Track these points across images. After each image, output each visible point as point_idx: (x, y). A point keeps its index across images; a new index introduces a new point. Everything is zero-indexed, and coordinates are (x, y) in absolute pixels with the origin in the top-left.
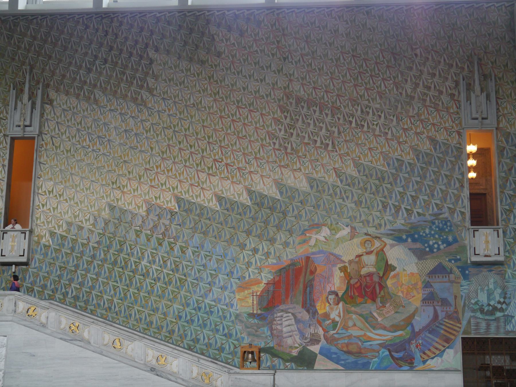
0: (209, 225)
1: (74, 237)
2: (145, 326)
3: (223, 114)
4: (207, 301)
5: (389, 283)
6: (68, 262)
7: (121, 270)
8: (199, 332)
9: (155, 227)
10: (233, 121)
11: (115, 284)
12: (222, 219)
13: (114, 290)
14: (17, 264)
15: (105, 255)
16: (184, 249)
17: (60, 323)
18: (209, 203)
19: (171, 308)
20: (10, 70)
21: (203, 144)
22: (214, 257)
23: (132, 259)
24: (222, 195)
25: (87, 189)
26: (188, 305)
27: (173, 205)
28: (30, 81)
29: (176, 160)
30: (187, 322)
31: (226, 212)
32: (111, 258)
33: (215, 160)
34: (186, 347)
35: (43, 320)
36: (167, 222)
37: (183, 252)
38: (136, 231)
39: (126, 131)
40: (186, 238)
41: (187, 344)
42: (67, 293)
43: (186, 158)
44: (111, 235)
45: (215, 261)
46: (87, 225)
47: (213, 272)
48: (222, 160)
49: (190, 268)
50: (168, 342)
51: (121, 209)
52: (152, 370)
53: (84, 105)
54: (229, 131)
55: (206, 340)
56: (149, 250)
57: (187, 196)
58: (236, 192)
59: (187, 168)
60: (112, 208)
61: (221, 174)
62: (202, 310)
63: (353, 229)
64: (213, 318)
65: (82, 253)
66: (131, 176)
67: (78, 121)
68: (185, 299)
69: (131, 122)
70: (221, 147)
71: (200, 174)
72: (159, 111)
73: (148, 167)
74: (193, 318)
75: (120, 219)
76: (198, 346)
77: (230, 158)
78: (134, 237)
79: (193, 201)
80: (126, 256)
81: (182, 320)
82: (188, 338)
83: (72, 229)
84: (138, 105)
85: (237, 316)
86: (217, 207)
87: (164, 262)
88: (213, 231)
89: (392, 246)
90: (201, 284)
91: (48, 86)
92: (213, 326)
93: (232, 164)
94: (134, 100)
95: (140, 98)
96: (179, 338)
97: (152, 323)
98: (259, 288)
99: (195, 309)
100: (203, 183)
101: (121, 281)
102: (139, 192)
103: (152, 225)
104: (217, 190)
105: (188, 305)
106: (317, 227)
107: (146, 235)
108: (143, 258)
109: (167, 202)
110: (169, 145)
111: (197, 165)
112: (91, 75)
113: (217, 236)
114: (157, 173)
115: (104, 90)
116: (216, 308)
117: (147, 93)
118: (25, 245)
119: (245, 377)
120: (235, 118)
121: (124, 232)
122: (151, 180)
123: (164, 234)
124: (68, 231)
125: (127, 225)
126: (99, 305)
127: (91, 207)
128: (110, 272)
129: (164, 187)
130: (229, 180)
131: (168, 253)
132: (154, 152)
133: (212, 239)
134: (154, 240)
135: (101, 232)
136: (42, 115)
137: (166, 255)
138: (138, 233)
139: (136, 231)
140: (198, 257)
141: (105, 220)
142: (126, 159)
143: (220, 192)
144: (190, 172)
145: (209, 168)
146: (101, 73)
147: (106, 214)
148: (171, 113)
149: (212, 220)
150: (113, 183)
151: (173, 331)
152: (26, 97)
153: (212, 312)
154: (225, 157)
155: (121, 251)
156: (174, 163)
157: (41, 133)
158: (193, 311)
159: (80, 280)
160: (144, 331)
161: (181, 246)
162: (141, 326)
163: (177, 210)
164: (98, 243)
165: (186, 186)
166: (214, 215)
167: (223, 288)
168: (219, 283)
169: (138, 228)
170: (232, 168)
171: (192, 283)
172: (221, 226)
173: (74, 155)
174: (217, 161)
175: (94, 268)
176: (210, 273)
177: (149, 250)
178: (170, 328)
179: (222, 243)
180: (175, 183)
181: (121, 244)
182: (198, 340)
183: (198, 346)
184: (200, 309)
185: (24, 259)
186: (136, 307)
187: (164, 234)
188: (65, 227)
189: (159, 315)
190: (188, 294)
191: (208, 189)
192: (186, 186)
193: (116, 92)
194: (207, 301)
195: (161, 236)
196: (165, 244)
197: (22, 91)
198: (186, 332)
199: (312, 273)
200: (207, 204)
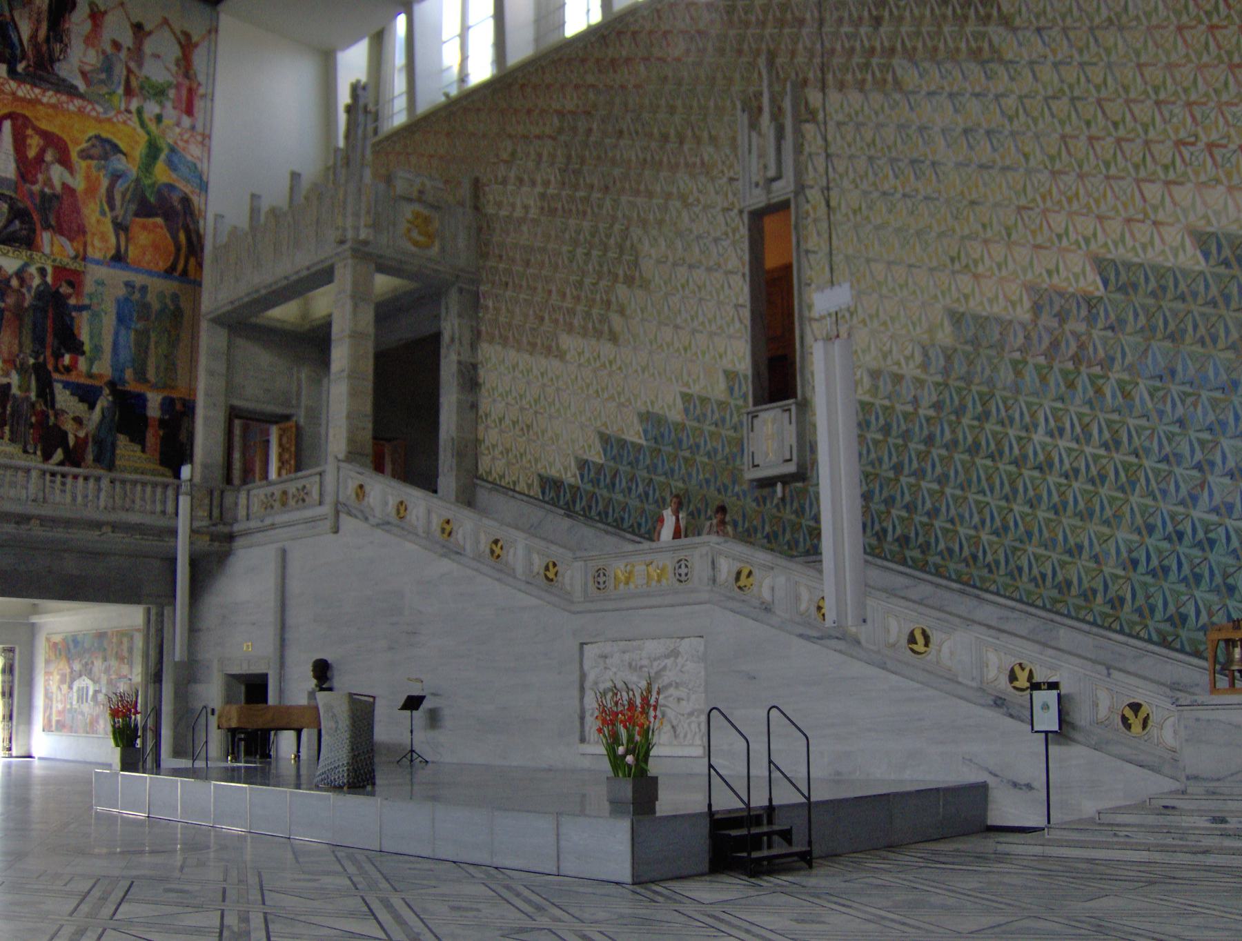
0: (1181, 315)
1: (887, 403)
2: (1054, 593)
3: (1185, 19)
4: (1196, 514)
6: (880, 461)
7: (989, 462)
8: (1184, 598)
9: (1055, 345)
10: (1212, 28)
11: (980, 497)
12: (1214, 291)
13: (980, 512)
14: (785, 479)
15: (953, 432)
16: (1129, 388)
17: (798, 598)
18: (1176, 256)
19: (1112, 542)
20: (737, 76)
21: (1144, 111)
22: (1205, 395)
24: (1210, 229)
25: (901, 287)
26: (1151, 529)
27: (1091, 283)
28: (770, 85)
29: (1086, 168)
30: (1153, 573)
31: (1222, 270)
32: (965, 438)
33: (1180, 143)
34: (1155, 637)
35: (766, 595)
36: (1081, 327)
37: (1126, 395)
38: (1015, 363)
39: (966, 132)
40: (1129, 359)
41: (1158, 631)
42: (885, 531)
43: (1109, 156)
44: (962, 384)
45: (1206, 403)
46: (911, 370)
47: (1206, 436)
48: (1196, 136)
49: (1148, 432)
50: (1109, 628)
51: (976, 318)
52: (999, 702)
53: (876, 98)
54: (1205, 59)
55: (1204, 618)
56: (1047, 404)
57: (1121, 250)
59: (1112, 182)
60: (957, 319)
61: (1197, 174)
62: (1187, 540)
64: (1218, 557)
65: (906, 435)
66: (989, 234)
67: (869, 139)
68: (1142, 516)
69: (974, 106)
70: (1189, 104)
71: (1146, 187)
72: (1031, 63)
73: (1023, 202)
74: (1166, 562)
75: (975, 342)
76: (1183, 634)
77: (1217, 127)
79: (1136, 260)
80: (998, 428)
81: (1142, 568)
82: (1159, 615)
83: (881, 384)
84: (983, 63)
86: (1198, 263)
87: (1085, 428)
88: (1195, 327)
90: (1178, 470)
91: (805, 82)
92: (1218, 579)
93: (1224, 141)
94: (975, 54)
95: (986, 46)
96: (1136, 618)
97: (1069, 584)
99: (1168, 538)
100: (1155, 208)
101: (992, 490)
102: (1011, 266)
103: (1046, 342)
104: (1192, 218)
105: (1151, 529)
107: (1037, 367)
108: (1036, 426)
109: (1076, 277)
111: (1136, 167)
112: (882, 30)
113: (1207, 339)
115: (910, 55)
116: (1221, 531)
117: (1001, 30)
118: (791, 437)
119: (1222, 715)
120: (1215, 20)
121: (987, 372)
122: (1033, 233)
123: (1077, 360)
124: (875, 390)
125: (993, 352)
126: (950, 551)
127: (914, 324)
128: (967, 471)
129: (1065, 243)
130: (1222, 183)
131: (1090, 402)
132: (1032, 163)
133: (1193, 348)
134: (1054, 378)
135: (939, 379)
136: (798, 149)
137: (1086, 410)
139: (1015, 363)
140: (1165, 403)
141: (944, 350)
142: (974, 196)
143: (1202, 223)
144: (1120, 188)
145: (1166, 168)
146: (901, 19)
147: (945, 336)
148: (1059, 57)
149: (1189, 299)
150: (952, 260)
151: (1122, 600)
152: (765, 119)
153: (1212, 543)
154: (1203, 128)
155: (984, 416)
156: (1081, 176)
157: (800, 188)
158: (1165, 545)
159: (907, 498)
160: (1051, 607)
161: (1119, 382)
162: (1045, 593)
163: (1100, 291)
164: (938, 406)
165: (1115, 226)
166: (1193, 285)
168: (1224, 463)
169: (1017, 355)
170: (1224, 151)
171: (1157, 472)
172: (1213, 311)
173: (867, 218)
174: (1185, 144)
175: (934, 466)
176: (1198, 440)
177: (1047, 404)
178: (1111, 593)
179: (1222, 355)
180: (1087, 225)
181: (985, 399)
182: (1184, 619)
183: (1183, 634)
184: (1180, 535)
185: (791, 468)
186: (1030, 549)
187: (1077, 360)
188: (867, 381)
189: (1085, 562)
190: (1149, 501)
191: (1170, 220)
192: (1115, 226)
193: (936, 49)
194: (1196, 514)
195: (1070, 366)
196: (1082, 381)
197: (760, 109)
198: (1152, 601)
200: (1172, 259)
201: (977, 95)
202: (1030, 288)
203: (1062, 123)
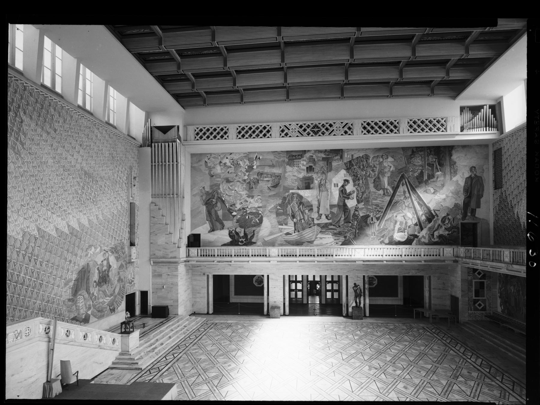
5: (110, 273)
9: (27, 248)
23: (16, 273)
27: (35, 233)
36: (33, 245)
37: (41, 265)
38: (17, 252)
58: (63, 226)
63: (101, 247)
66: (13, 210)
78: (16, 256)
85: (64, 302)
89: (111, 255)
98: (71, 284)
102: (18, 222)
106: (90, 246)
110: (33, 189)
114: (27, 209)
123: (32, 254)
125: (12, 247)
131: (34, 267)
138: (18, 253)
139: (17, 252)
167: (58, 286)
187: (32, 254)
196: (32, 260)
199: (89, 272)
201: (13, 162)
202: (22, 230)
203: (33, 185)
